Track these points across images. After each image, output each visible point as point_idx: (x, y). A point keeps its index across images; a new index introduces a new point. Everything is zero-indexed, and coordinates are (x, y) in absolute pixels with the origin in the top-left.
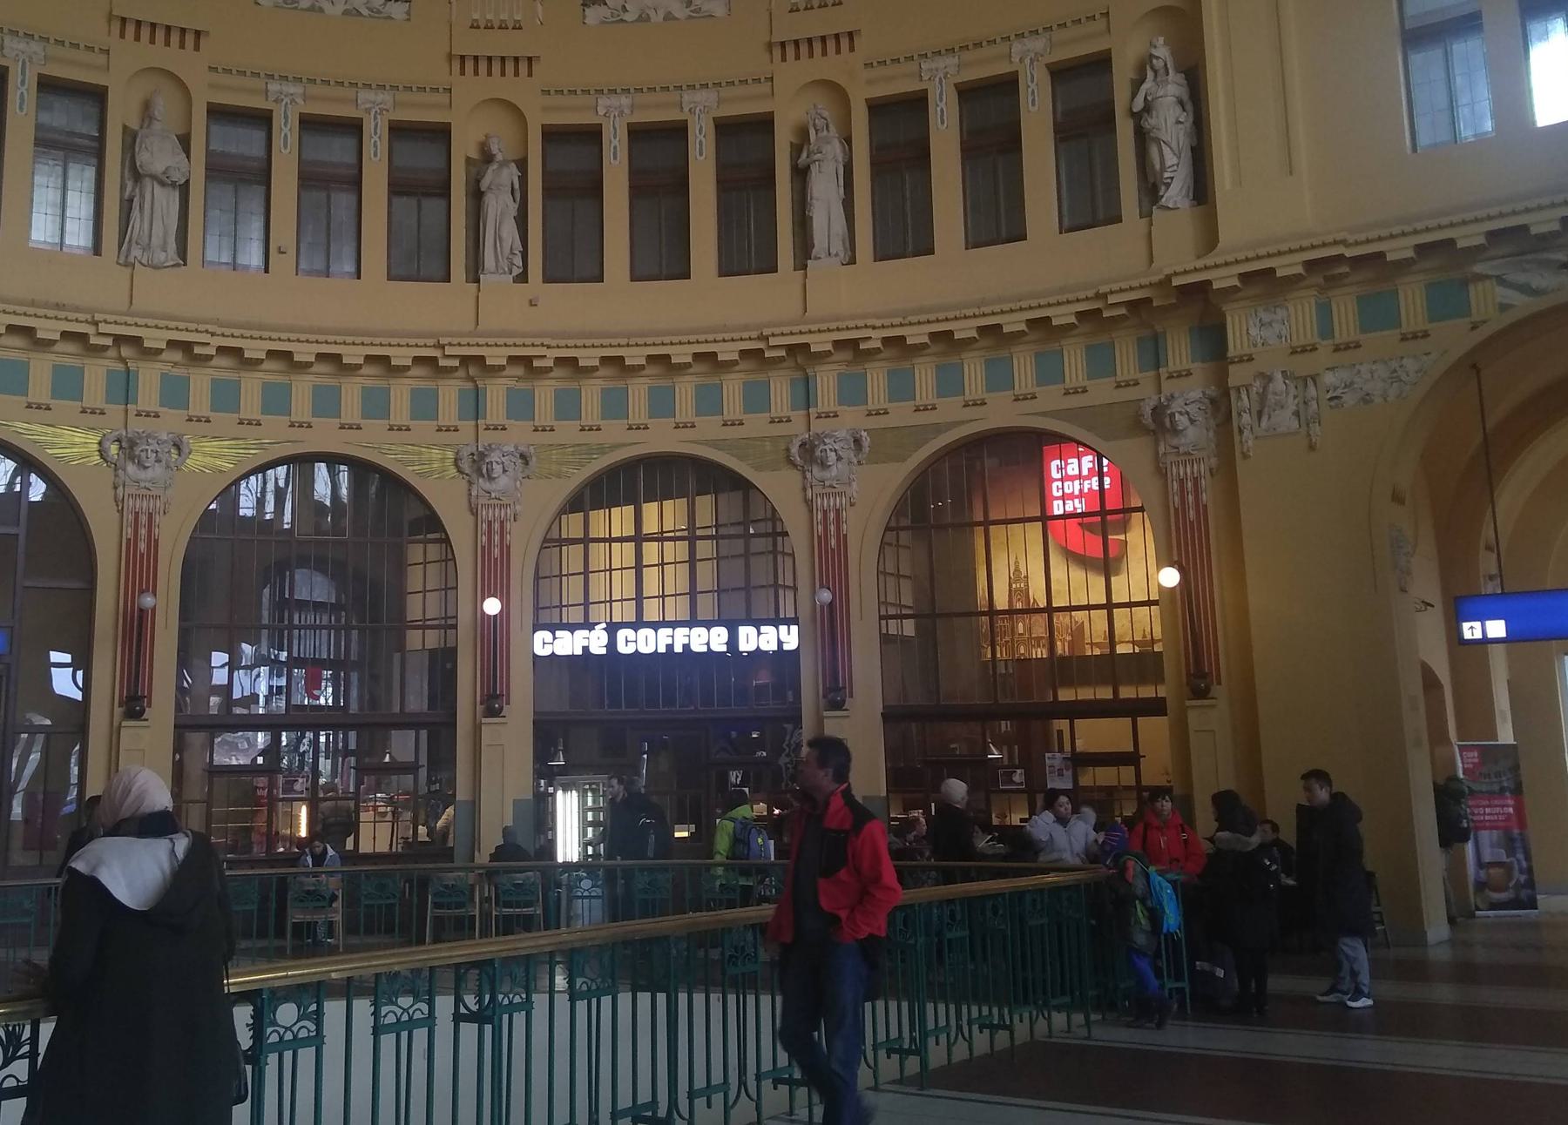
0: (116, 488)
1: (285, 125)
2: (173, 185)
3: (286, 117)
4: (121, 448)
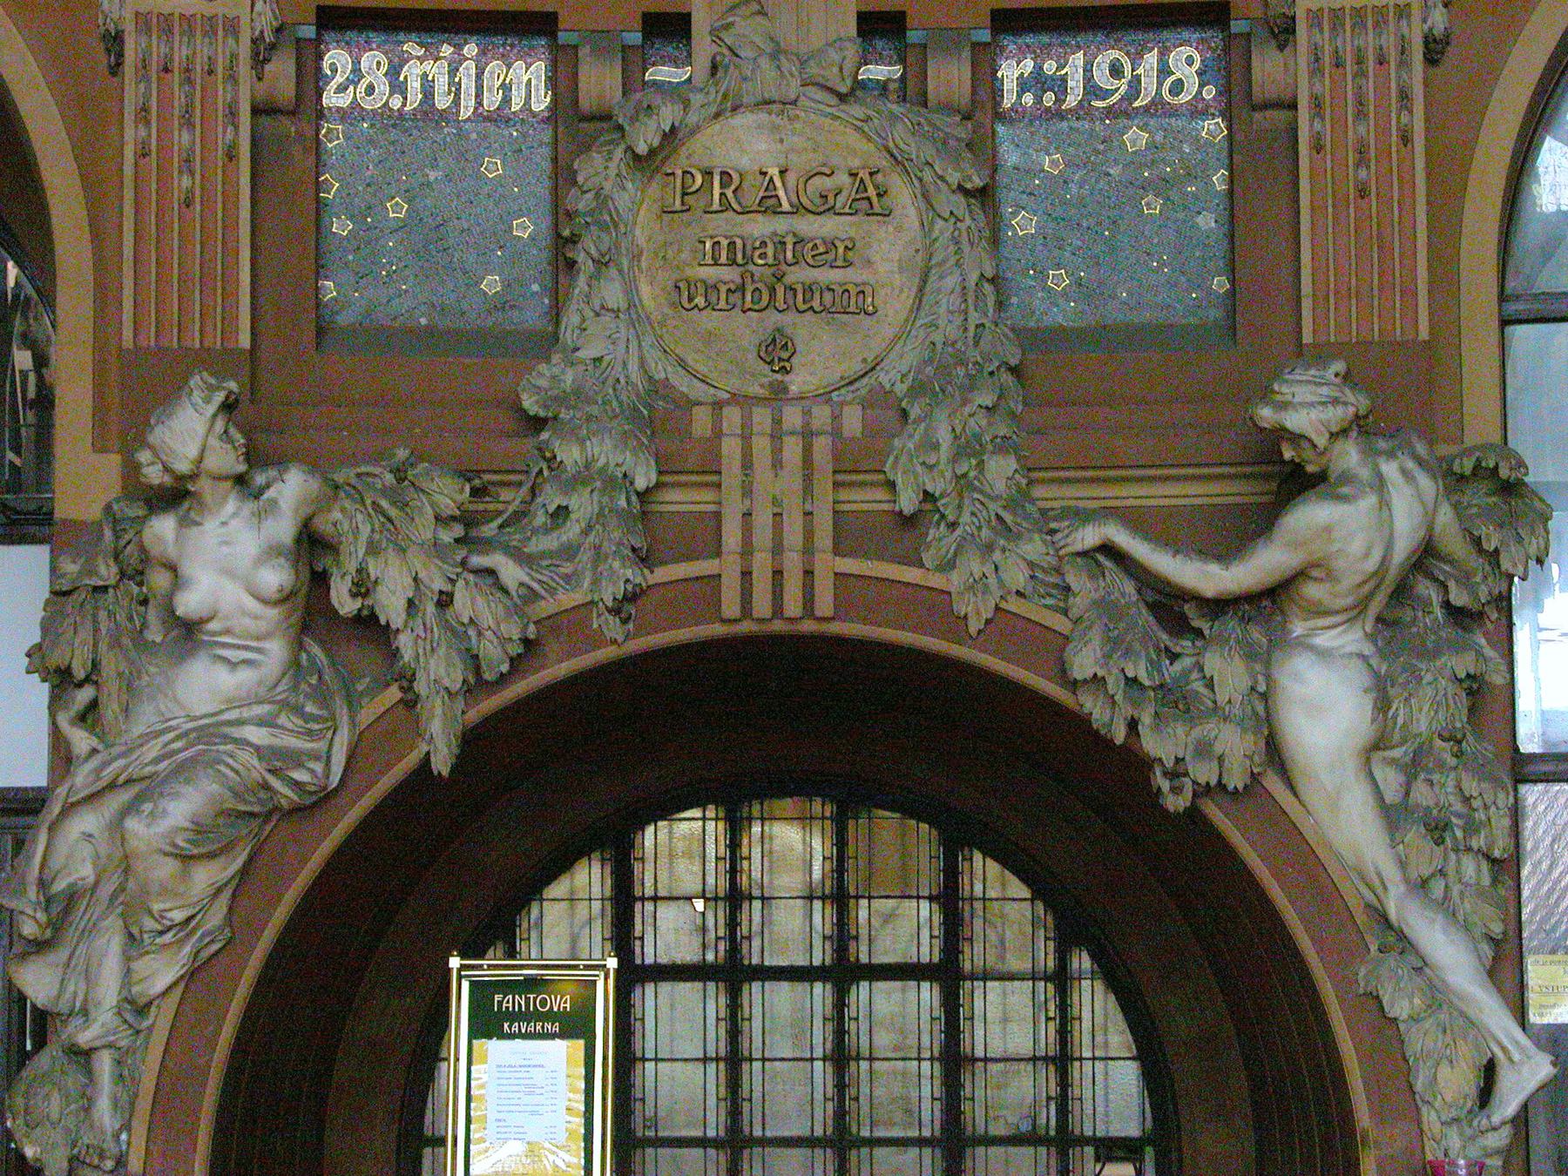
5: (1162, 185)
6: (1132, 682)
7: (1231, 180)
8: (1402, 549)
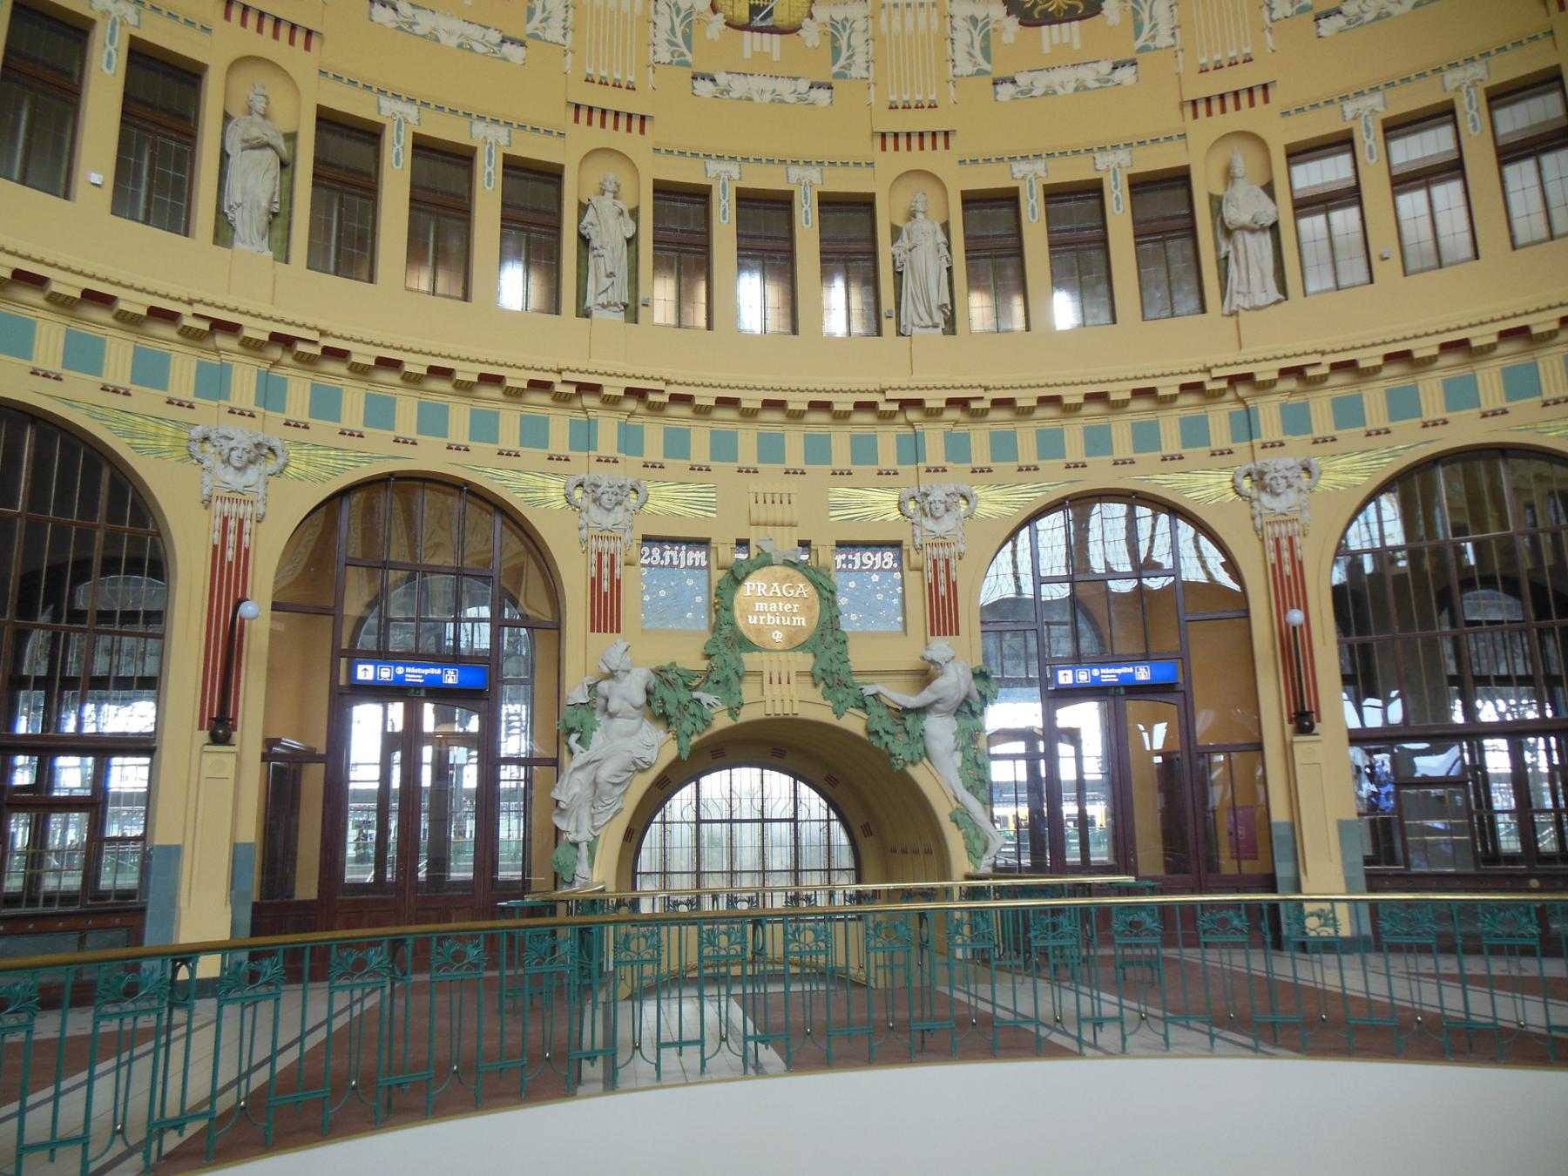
0: (1253, 518)
1: (1368, 137)
2: (1263, 229)
3: (1368, 129)
4: (1253, 481)
5: (885, 592)
6: (887, 732)
7: (903, 590)
8: (962, 696)
